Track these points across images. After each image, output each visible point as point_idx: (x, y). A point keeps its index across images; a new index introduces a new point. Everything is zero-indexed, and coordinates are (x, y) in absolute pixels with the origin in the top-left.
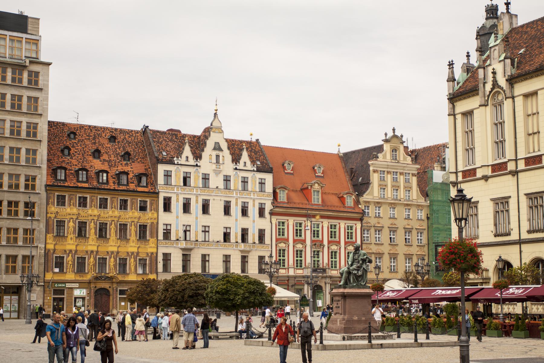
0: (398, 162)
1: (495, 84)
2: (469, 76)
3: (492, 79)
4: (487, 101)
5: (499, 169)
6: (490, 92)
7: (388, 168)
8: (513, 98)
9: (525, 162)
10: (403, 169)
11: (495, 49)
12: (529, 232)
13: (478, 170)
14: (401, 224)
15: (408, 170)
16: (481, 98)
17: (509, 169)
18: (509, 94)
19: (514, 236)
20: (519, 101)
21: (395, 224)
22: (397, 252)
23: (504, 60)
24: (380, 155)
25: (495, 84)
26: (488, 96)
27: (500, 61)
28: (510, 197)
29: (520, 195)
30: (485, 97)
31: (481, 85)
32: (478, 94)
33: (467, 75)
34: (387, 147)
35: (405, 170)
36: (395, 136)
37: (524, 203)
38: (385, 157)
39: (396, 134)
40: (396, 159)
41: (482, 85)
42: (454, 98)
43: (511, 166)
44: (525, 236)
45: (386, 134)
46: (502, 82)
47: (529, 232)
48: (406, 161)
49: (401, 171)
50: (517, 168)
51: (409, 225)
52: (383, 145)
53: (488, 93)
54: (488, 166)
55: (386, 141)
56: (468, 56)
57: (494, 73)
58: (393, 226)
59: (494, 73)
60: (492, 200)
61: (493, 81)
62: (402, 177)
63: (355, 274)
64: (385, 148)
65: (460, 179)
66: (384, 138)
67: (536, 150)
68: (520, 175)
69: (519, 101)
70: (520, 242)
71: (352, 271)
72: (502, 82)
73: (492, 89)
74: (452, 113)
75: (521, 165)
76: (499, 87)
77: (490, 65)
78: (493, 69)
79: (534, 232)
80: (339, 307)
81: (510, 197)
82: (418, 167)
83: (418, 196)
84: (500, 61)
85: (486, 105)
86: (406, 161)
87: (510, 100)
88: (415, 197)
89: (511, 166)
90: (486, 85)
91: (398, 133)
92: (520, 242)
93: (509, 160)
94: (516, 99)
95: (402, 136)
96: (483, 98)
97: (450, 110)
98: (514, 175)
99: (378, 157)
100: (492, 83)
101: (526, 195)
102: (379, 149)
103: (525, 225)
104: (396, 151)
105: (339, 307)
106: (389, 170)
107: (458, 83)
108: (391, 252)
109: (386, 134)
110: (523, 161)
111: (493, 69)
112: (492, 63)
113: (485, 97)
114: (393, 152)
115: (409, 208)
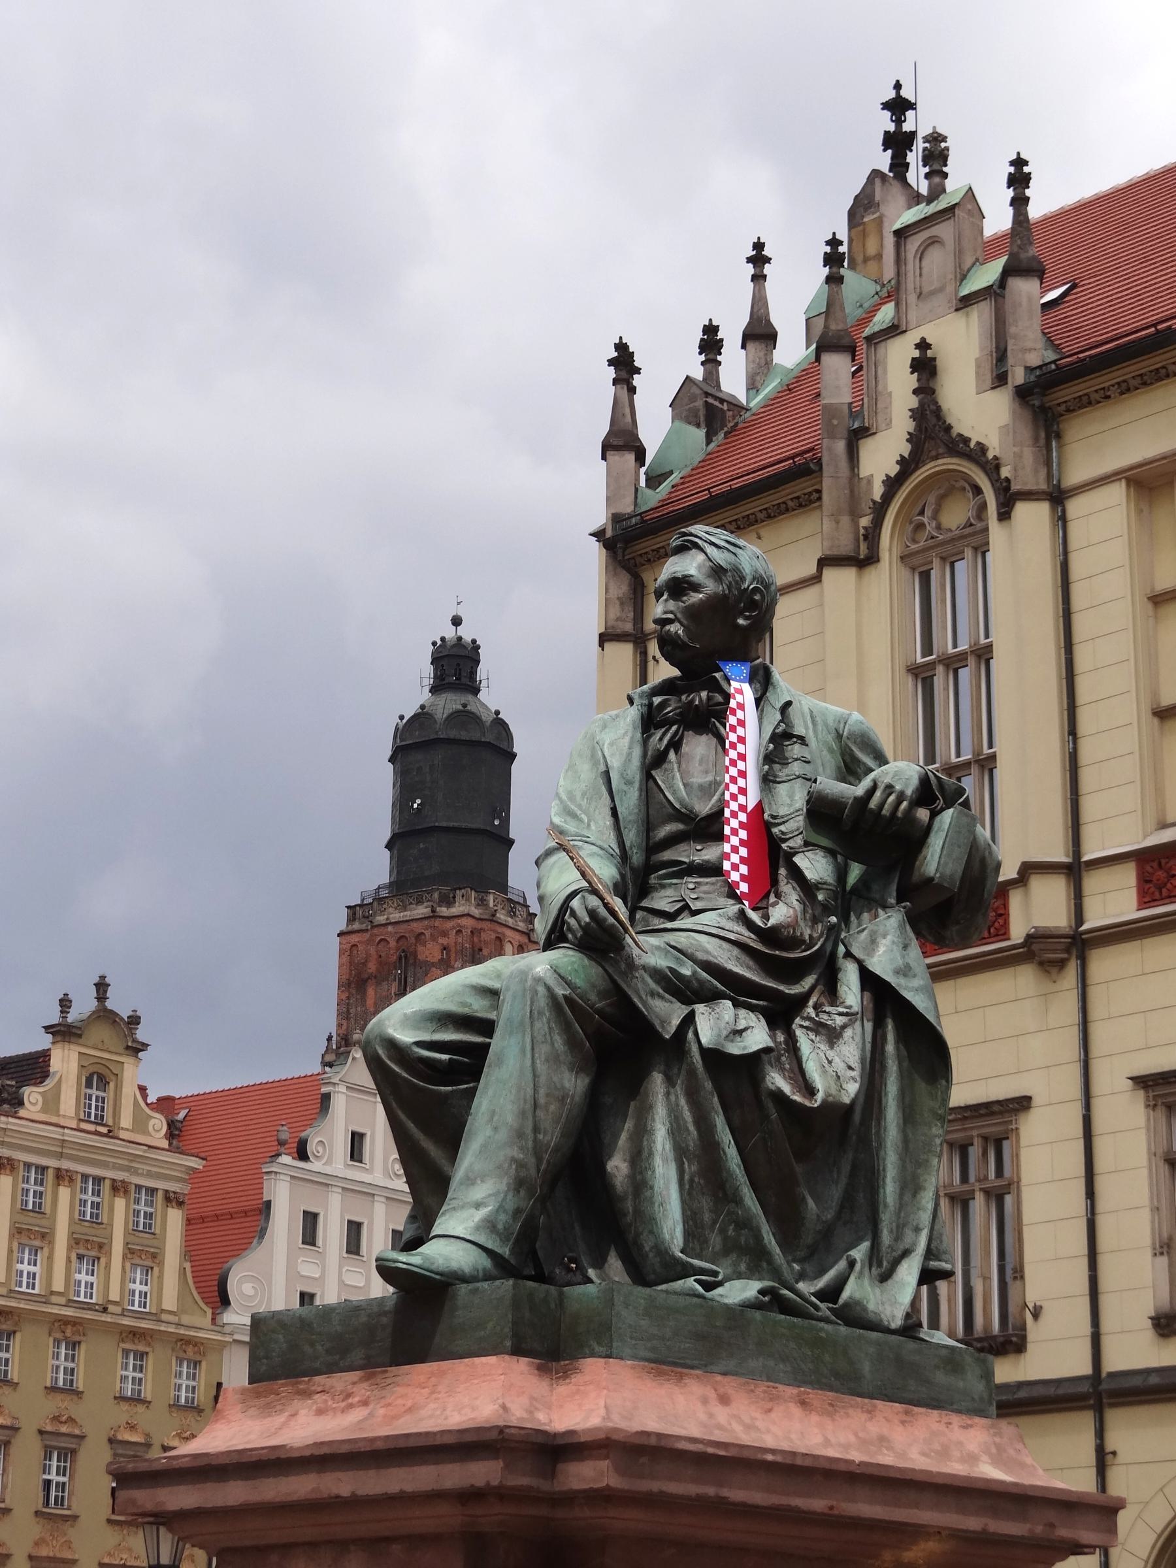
0: (110, 1134)
1: (931, 429)
2: (712, 445)
3: (914, 402)
4: (872, 536)
6: (893, 485)
7: (60, 1156)
8: (1058, 497)
10: (127, 1169)
11: (934, 241)
14: (97, 1419)
15: (150, 1175)
16: (835, 517)
17: (1018, 932)
19: (1054, 1353)
20: (1102, 519)
21: (71, 1420)
22: (68, 1555)
23: (996, 292)
24: (32, 1095)
25: (931, 429)
27: (966, 302)
28: (1023, 1103)
29: (1097, 1087)
30: (855, 515)
32: (811, 501)
33: (709, 441)
34: (65, 1063)
35: (136, 1172)
36: (104, 1015)
38: (52, 1102)
39: (109, 1004)
40: (100, 1121)
41: (840, 446)
43: (1040, 909)
44: (1134, 1349)
45: (65, 1003)
46: (982, 414)
48: (146, 1132)
49: (119, 1175)
50: (1079, 917)
51: (132, 1427)
52: (45, 1055)
53: (878, 492)
55: (63, 1032)
56: (711, 343)
57: (925, 366)
58: (64, 1429)
59: (925, 366)
61: (918, 415)
62: (120, 1203)
63: (735, 1073)
64: (56, 1064)
66: (54, 1018)
68: (1105, 965)
69: (1102, 519)
71: (668, 1014)
72: (982, 414)
73: (907, 466)
74: (628, 627)
75: (1114, 900)
76: (960, 447)
77: (894, 330)
78: (923, 345)
81: (1023, 1103)
82: (195, 1163)
83: (180, 1298)
84: (966, 302)
86: (146, 1132)
87: (1033, 517)
88: (170, 1301)
89: (1040, 909)
91: (119, 1003)
93: (1028, 870)
94: (1075, 507)
95: (135, 1020)
96: (845, 520)
97: (615, 611)
98: (1051, 966)
99: (21, 1103)
100: (910, 426)
101: (1143, 1082)
102: (34, 1067)
104: (103, 1082)
106: (65, 1164)
107: (654, 480)
108: (44, 1552)
109: (65, 1003)
110: (1127, 878)
111: (923, 345)
112: (913, 316)
113: (855, 515)
114: (89, 1084)
115: (141, 1348)
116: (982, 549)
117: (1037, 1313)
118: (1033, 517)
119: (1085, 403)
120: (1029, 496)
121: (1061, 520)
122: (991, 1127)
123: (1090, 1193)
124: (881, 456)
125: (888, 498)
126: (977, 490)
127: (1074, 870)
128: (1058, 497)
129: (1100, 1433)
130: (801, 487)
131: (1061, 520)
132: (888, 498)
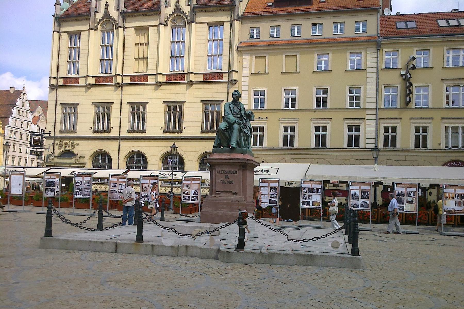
1: (107, 14)
5: (104, 81)
9: (131, 79)
12: (129, 131)
13: (80, 79)
18: (121, 24)
19: (114, 133)
25: (107, 14)
26: (98, 23)
31: (92, 13)
37: (127, 109)
42: (60, 20)
44: (124, 133)
47: (129, 131)
54: (92, 77)
59: (107, 5)
60: (93, 104)
65: (61, 83)
67: (141, 70)
70: (120, 138)
72: (114, 14)
74: (58, 30)
75: (127, 80)
76: (111, 18)
79: (134, 132)
80: (231, 183)
85: (96, 30)
87: (121, 30)
90: (97, 14)
92: (120, 138)
101: (129, 103)
103: (126, 126)
105: (231, 183)
116: (113, 32)
117: (112, 128)
118: (121, 30)
119: (129, 16)
120: (120, 27)
121: (124, 31)
122: (108, 105)
123: (121, 115)
124: (99, 16)
125: (99, 22)
126: (113, 24)
127: (122, 76)
128: (124, 28)
129: (119, 143)
130: (87, 17)
131: (124, 31)
132: (99, 22)
